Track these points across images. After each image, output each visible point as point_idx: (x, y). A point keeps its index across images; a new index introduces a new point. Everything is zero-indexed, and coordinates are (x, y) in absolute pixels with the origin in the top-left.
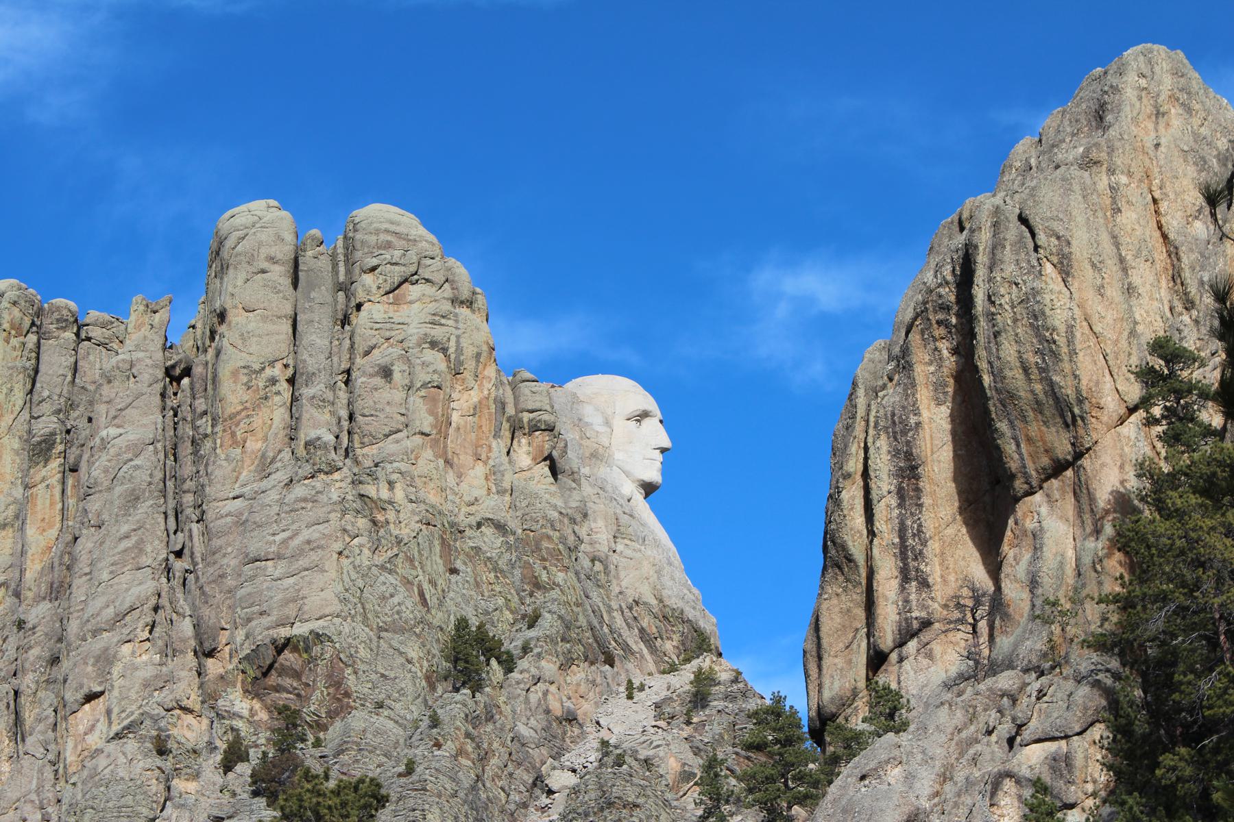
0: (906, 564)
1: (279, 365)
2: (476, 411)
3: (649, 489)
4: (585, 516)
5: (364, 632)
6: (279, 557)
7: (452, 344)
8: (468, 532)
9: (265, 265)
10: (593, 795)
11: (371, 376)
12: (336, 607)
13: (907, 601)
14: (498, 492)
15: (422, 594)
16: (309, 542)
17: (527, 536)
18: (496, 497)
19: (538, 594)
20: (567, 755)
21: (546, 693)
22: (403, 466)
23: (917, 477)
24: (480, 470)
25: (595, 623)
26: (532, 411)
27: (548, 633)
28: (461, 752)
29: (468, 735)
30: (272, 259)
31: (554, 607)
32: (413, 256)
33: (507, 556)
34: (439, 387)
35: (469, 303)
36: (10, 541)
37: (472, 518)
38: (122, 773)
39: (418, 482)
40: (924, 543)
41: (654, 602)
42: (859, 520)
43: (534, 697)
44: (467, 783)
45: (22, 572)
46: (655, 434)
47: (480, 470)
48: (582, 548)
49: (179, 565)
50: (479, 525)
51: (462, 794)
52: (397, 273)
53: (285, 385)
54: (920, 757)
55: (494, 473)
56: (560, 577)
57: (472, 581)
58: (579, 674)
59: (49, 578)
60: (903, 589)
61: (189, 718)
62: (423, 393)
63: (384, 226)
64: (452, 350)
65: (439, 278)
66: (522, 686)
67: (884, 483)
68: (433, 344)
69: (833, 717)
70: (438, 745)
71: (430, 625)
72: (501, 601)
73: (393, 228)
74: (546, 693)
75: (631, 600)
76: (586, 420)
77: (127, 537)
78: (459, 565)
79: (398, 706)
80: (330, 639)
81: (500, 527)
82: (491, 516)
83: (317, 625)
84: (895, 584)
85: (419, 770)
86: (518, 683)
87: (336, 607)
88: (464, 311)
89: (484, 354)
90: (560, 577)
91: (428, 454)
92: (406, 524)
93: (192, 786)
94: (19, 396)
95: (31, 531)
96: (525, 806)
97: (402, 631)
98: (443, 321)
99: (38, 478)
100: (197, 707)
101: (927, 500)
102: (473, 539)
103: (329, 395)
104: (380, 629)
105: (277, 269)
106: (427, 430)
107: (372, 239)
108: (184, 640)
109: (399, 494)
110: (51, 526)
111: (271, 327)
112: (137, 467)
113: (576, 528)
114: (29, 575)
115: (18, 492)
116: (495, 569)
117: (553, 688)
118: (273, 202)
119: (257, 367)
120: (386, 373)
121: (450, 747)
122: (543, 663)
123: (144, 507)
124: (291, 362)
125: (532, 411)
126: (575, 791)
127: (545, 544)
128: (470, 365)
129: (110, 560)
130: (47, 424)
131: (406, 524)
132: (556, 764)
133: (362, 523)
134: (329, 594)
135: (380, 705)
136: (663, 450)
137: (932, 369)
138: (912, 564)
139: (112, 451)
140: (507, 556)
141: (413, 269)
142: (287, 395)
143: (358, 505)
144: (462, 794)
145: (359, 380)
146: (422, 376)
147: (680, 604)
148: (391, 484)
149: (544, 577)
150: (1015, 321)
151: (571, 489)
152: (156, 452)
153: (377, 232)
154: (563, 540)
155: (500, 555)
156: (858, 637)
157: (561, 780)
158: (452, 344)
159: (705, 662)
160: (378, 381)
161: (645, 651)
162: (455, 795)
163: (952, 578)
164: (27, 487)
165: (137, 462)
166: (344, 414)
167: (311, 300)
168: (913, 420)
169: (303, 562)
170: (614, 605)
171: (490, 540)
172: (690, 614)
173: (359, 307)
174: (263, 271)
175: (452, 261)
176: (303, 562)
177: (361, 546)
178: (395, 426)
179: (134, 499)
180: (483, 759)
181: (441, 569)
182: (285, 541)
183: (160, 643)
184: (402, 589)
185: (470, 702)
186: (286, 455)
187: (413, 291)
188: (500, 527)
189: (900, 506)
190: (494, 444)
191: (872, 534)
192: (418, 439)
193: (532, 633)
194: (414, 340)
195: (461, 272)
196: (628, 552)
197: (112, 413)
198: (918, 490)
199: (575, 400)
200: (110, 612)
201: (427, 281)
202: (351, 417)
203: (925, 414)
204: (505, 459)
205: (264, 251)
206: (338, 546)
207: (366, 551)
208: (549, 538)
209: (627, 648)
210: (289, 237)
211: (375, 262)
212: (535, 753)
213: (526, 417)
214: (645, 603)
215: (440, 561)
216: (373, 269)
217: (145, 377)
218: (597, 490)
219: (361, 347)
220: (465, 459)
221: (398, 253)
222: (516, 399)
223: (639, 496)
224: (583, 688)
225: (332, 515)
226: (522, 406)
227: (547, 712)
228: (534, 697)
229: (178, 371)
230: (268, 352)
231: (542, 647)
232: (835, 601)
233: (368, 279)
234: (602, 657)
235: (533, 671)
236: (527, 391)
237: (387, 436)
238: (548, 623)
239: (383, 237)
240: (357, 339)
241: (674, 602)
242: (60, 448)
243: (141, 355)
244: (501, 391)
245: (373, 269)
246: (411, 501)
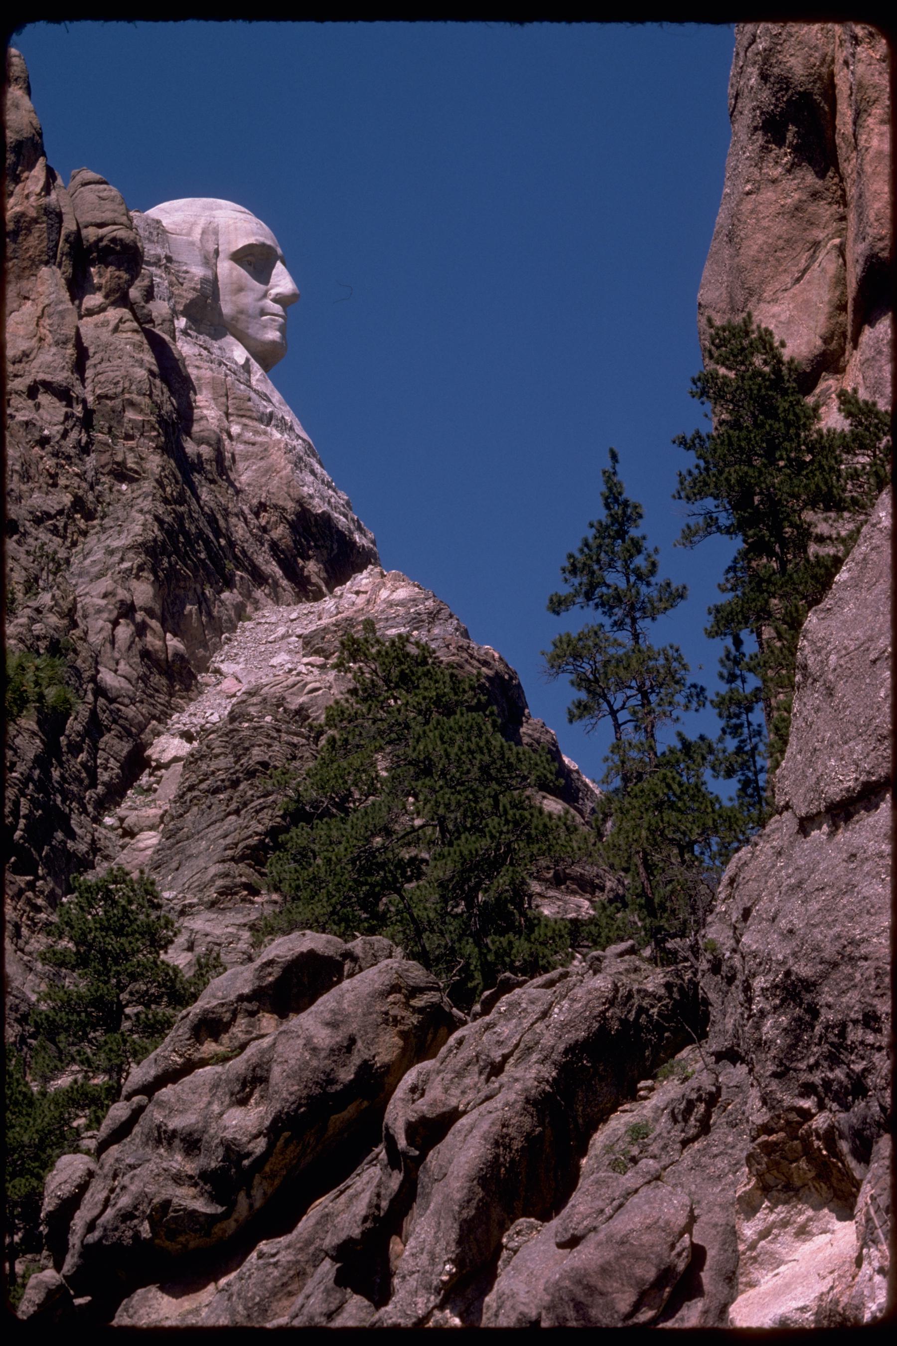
14: (57, 343)
17: (106, 405)
18: (54, 350)
20: (175, 716)
26: (101, 225)
27: (140, 539)
31: (147, 504)
37: (19, 379)
41: (290, 505)
66: (105, 615)
69: (618, 594)
75: (255, 502)
76: (175, 257)
82: (48, 378)
86: (99, 611)
116: (55, 455)
125: (101, 225)
132: (161, 728)
147: (326, 508)
155: (65, 435)
156: (821, 255)
161: (279, 572)
188: (63, 394)
196: (249, 435)
212: (130, 711)
214: (276, 507)
218: (196, 350)
226: (88, 218)
227: (145, 654)
231: (132, 560)
235: (122, 594)
241: (319, 507)
244: (53, 195)
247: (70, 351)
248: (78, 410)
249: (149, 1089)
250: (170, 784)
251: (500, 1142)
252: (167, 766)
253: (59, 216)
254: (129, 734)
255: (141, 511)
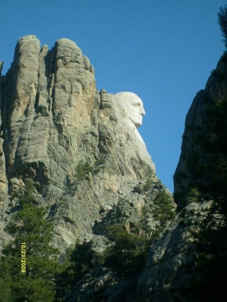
25: (120, 163)
34: (79, 93)
50: (87, 133)
57: (85, 150)
63: (65, 45)
90: (111, 149)
98: (81, 74)
107: (62, 49)
113: (116, 136)
117: (107, 182)
120: (63, 88)
124: (37, 83)
149: (106, 149)
151: (115, 125)
153: (64, 46)
170: (126, 159)
190: (94, 110)
194: (73, 78)
201: (77, 62)
204: (96, 115)
212: (100, 200)
213: (104, 103)
215: (76, 143)
222: (101, 98)
224: (115, 182)
226: (102, 100)
227: (105, 188)
236: (104, 96)
237: (63, 106)
246: (69, 125)
247: (97, 126)
248: (98, 138)
252: (106, 211)
254: (100, 204)
255: (107, 160)
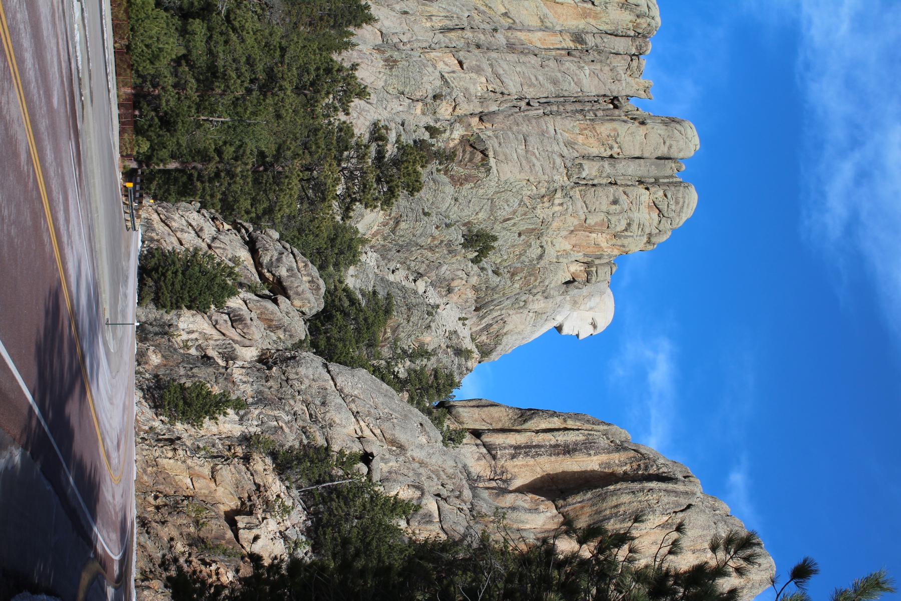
0: (522, 448)
1: (619, 150)
2: (597, 245)
3: (559, 329)
4: (546, 298)
5: (491, 192)
6: (527, 152)
7: (629, 234)
8: (538, 242)
9: (667, 144)
10: (414, 301)
11: (614, 195)
12: (503, 179)
13: (505, 448)
15: (509, 219)
16: (534, 165)
19: (509, 275)
21: (461, 278)
22: (570, 210)
23: (564, 454)
24: (568, 247)
25: (495, 302)
28: (434, 238)
29: (442, 241)
30: (670, 147)
31: (502, 283)
32: (672, 214)
33: (527, 260)
35: (649, 242)
36: (535, 24)
38: (425, 79)
39: (562, 218)
40: (533, 457)
41: (505, 331)
42: (544, 426)
43: (460, 273)
44: (419, 241)
45: (520, 30)
46: (586, 332)
47: (568, 247)
48: (531, 296)
49: (523, 104)
50: (542, 247)
51: (414, 239)
52: (663, 207)
53: (609, 154)
54: (431, 452)
55: (567, 254)
56: (517, 286)
58: (471, 295)
59: (517, 43)
60: (511, 446)
61: (451, 110)
62: (606, 220)
64: (626, 233)
65: (661, 227)
67: (561, 438)
68: (629, 225)
70: (437, 227)
71: (494, 223)
72: (505, 257)
73: (686, 205)
74: (461, 278)
77: (537, 79)
78: (523, 237)
79: (456, 208)
80: (487, 176)
81: (541, 257)
83: (494, 170)
84: (513, 443)
85: (426, 218)
87: (503, 179)
88: (645, 239)
89: (624, 249)
90: (517, 286)
91: (576, 222)
92: (542, 212)
93: (419, 111)
94: (604, 27)
95: (540, 34)
96: (409, 269)
97: (491, 210)
99: (565, 37)
100: (456, 113)
101: (553, 458)
102: (535, 244)
103: (604, 175)
104: (492, 200)
105: (666, 150)
106: (588, 222)
107: (680, 195)
108: (487, 107)
109: (557, 208)
110: (542, 44)
111: (637, 146)
112: (570, 83)
114: (519, 34)
115: (558, 28)
116: (521, 254)
117: (464, 282)
118: (698, 147)
119: (618, 140)
120: (615, 202)
121: (436, 233)
122: (476, 277)
123: (551, 87)
126: (416, 293)
127: (533, 278)
128: (619, 242)
129: (526, 72)
130: (591, 41)
131: (542, 212)
133: (543, 191)
134: (509, 175)
135: (456, 200)
136: (578, 336)
137: (617, 462)
138: (523, 451)
139: (578, 72)
140: (527, 260)
141: (666, 215)
142: (604, 155)
143: (551, 189)
144: (414, 239)
145: (612, 189)
146: (614, 219)
148: (561, 204)
149: (517, 278)
150: (640, 502)
152: (577, 92)
153: (684, 198)
154: (534, 287)
157: (421, 286)
158: (629, 234)
159: (476, 355)
160: (611, 198)
162: (414, 235)
163: (516, 470)
164: (561, 32)
165: (572, 84)
166: (595, 182)
167: (651, 165)
168: (592, 452)
169: (524, 162)
170: (503, 312)
171: (535, 252)
172: (499, 348)
173: (647, 189)
174: (664, 143)
175: (669, 233)
176: (524, 162)
177: (532, 190)
178: (589, 206)
179: (555, 82)
180: (431, 249)
181: (521, 229)
182: (534, 154)
183: (486, 96)
184: (511, 210)
185: (457, 243)
186: (576, 154)
187: (655, 214)
188: (541, 257)
189: (551, 445)
191: (537, 432)
192: (583, 217)
193: (490, 272)
194: (631, 215)
195: (664, 238)
196: (528, 318)
197: (596, 72)
198: (558, 454)
199: (602, 293)
200: (501, 72)
202: (594, 185)
203: (595, 458)
205: (674, 143)
206: (532, 179)
207: (529, 193)
208: (536, 280)
209: (483, 317)
210: (681, 155)
211: (669, 196)
212: (433, 274)
213: (594, 269)
216: (666, 196)
217: (613, 87)
219: (628, 190)
220: (574, 240)
221: (673, 207)
223: (556, 324)
225: (546, 177)
226: (599, 267)
227: (453, 280)
228: (460, 273)
229: (616, 102)
230: (625, 146)
232: (505, 414)
233: (661, 193)
234: (478, 306)
235: (472, 273)
238: (495, 280)
239: (681, 200)
240: (632, 188)
241: (505, 340)
242: (579, 47)
243: (624, 85)
245: (666, 196)
249: (292, 253)
250: (410, 285)
251: (272, 313)
253: (599, 258)
